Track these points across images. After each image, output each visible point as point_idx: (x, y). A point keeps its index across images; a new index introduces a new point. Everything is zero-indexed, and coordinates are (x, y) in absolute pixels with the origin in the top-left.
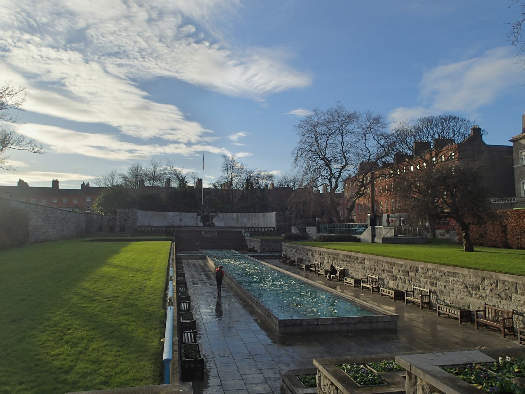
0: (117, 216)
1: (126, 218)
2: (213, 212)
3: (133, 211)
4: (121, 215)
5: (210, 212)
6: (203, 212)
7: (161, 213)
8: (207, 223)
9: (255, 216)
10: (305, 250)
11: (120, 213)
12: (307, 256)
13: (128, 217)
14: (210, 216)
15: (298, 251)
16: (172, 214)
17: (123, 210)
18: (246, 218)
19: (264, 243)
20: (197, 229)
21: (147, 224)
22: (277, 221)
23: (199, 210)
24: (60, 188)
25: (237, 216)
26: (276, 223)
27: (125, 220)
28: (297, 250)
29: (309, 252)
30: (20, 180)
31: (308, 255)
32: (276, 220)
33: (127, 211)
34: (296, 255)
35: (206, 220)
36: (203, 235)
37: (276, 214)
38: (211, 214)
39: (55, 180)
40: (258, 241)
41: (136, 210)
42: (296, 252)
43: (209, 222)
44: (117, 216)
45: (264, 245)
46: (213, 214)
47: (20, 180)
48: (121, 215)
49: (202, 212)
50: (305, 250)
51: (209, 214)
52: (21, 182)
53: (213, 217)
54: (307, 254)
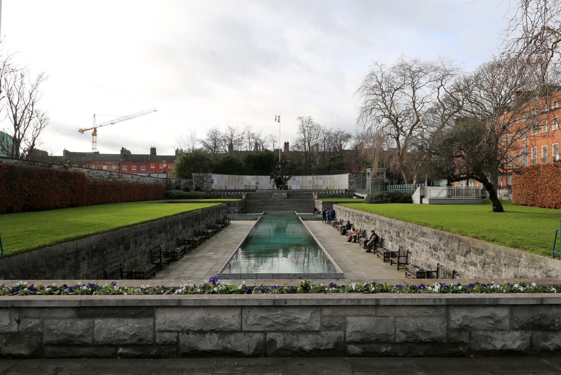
1: (201, 182)
2: (287, 175)
3: (207, 175)
4: (197, 179)
5: (284, 175)
6: (277, 175)
8: (280, 186)
11: (197, 177)
13: (203, 181)
14: (284, 179)
16: (249, 178)
17: (199, 174)
18: (322, 181)
19: (326, 205)
20: (270, 191)
21: (223, 188)
22: (350, 183)
24: (157, 154)
25: (313, 179)
26: (349, 184)
30: (123, 148)
32: (349, 182)
33: (201, 175)
35: (280, 183)
36: (273, 197)
37: (349, 176)
38: (284, 177)
40: (321, 203)
41: (211, 174)
43: (282, 185)
46: (287, 177)
47: (123, 148)
48: (197, 179)
49: (275, 175)
51: (283, 178)
52: (123, 150)
53: (287, 180)
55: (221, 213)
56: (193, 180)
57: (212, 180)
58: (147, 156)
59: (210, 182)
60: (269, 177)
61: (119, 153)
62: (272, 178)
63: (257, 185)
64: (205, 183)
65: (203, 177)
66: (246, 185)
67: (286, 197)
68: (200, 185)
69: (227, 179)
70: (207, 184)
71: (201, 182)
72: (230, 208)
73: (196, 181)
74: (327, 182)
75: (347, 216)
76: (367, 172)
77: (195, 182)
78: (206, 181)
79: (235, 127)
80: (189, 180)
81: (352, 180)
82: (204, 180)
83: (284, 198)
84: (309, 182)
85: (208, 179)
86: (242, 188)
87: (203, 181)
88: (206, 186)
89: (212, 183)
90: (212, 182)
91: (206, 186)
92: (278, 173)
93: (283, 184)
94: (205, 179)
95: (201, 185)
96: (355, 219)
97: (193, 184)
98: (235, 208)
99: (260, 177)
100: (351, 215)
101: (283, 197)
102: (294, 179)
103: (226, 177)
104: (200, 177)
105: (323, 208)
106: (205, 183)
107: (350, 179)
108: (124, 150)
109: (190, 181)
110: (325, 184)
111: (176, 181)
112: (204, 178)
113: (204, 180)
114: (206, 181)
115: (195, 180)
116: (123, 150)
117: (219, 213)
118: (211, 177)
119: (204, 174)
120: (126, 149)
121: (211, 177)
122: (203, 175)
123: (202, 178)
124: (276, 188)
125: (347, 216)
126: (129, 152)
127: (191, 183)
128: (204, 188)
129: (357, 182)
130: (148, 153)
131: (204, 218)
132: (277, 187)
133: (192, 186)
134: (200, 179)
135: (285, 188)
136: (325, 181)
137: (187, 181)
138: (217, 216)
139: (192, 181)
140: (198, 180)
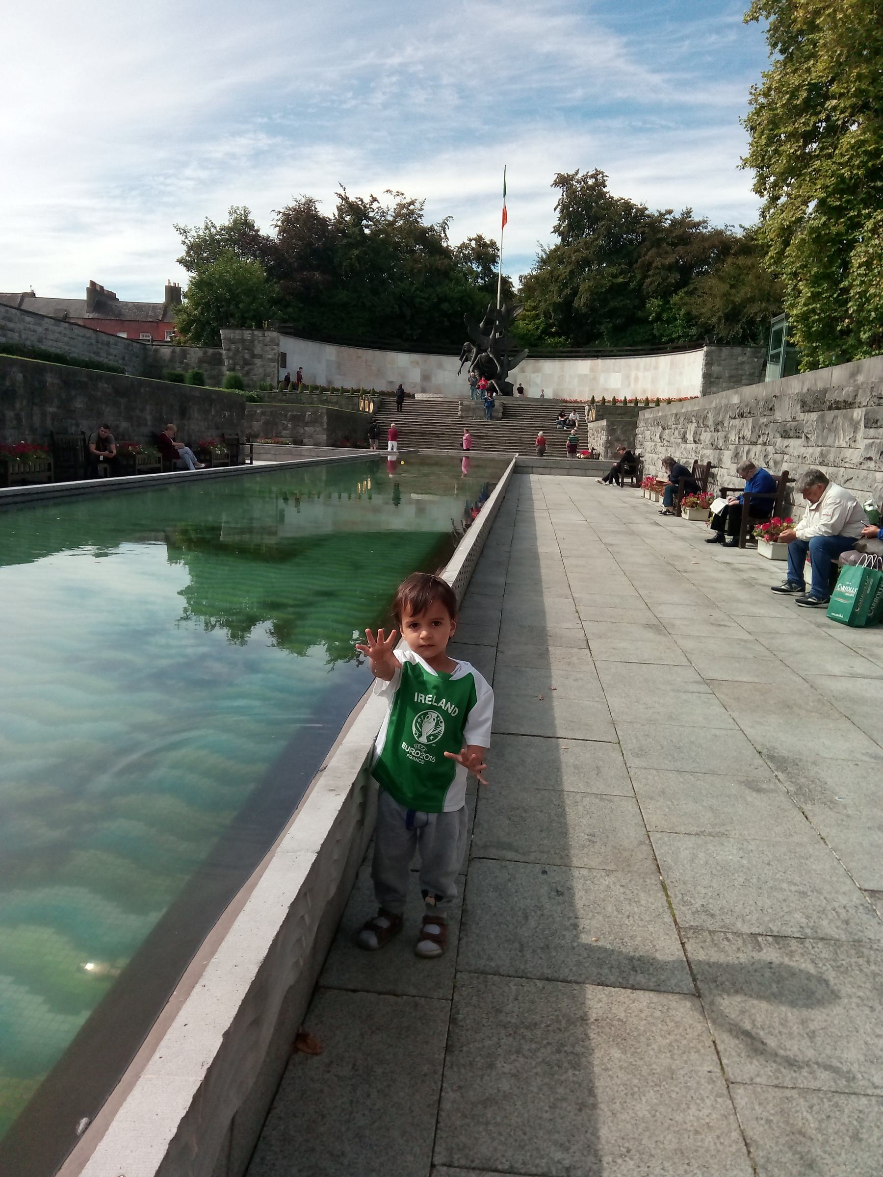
0: (221, 351)
1: (247, 356)
3: (264, 336)
9: (646, 369)
11: (232, 341)
12: (683, 445)
13: (254, 356)
17: (238, 332)
25: (592, 370)
27: (246, 363)
30: (93, 284)
33: (247, 334)
36: (459, 413)
37: (707, 355)
39: (172, 285)
44: (221, 351)
45: (618, 440)
47: (93, 284)
48: (233, 347)
52: (95, 291)
54: (684, 439)
57: (283, 356)
58: (154, 306)
59: (272, 360)
61: (83, 296)
62: (466, 360)
64: (258, 362)
65: (252, 341)
66: (391, 383)
68: (242, 367)
70: (263, 366)
72: (302, 431)
73: (231, 354)
74: (637, 379)
75: (690, 437)
76: (773, 329)
78: (260, 357)
79: (367, 200)
80: (210, 351)
81: (715, 368)
84: (582, 378)
85: (268, 348)
91: (261, 370)
94: (258, 350)
95: (246, 369)
97: (220, 362)
99: (433, 359)
100: (710, 422)
102: (537, 371)
103: (330, 352)
104: (243, 341)
105: (607, 441)
106: (258, 362)
107: (708, 364)
108: (98, 289)
109: (214, 354)
110: (629, 385)
111: (173, 352)
114: (260, 357)
115: (229, 350)
116: (95, 291)
119: (256, 333)
120: (102, 287)
122: (253, 334)
123: (249, 346)
125: (690, 437)
126: (112, 296)
127: (217, 360)
128: (255, 378)
129: (731, 377)
130: (160, 298)
133: (220, 370)
136: (628, 377)
137: (205, 353)
139: (221, 354)
140: (237, 350)
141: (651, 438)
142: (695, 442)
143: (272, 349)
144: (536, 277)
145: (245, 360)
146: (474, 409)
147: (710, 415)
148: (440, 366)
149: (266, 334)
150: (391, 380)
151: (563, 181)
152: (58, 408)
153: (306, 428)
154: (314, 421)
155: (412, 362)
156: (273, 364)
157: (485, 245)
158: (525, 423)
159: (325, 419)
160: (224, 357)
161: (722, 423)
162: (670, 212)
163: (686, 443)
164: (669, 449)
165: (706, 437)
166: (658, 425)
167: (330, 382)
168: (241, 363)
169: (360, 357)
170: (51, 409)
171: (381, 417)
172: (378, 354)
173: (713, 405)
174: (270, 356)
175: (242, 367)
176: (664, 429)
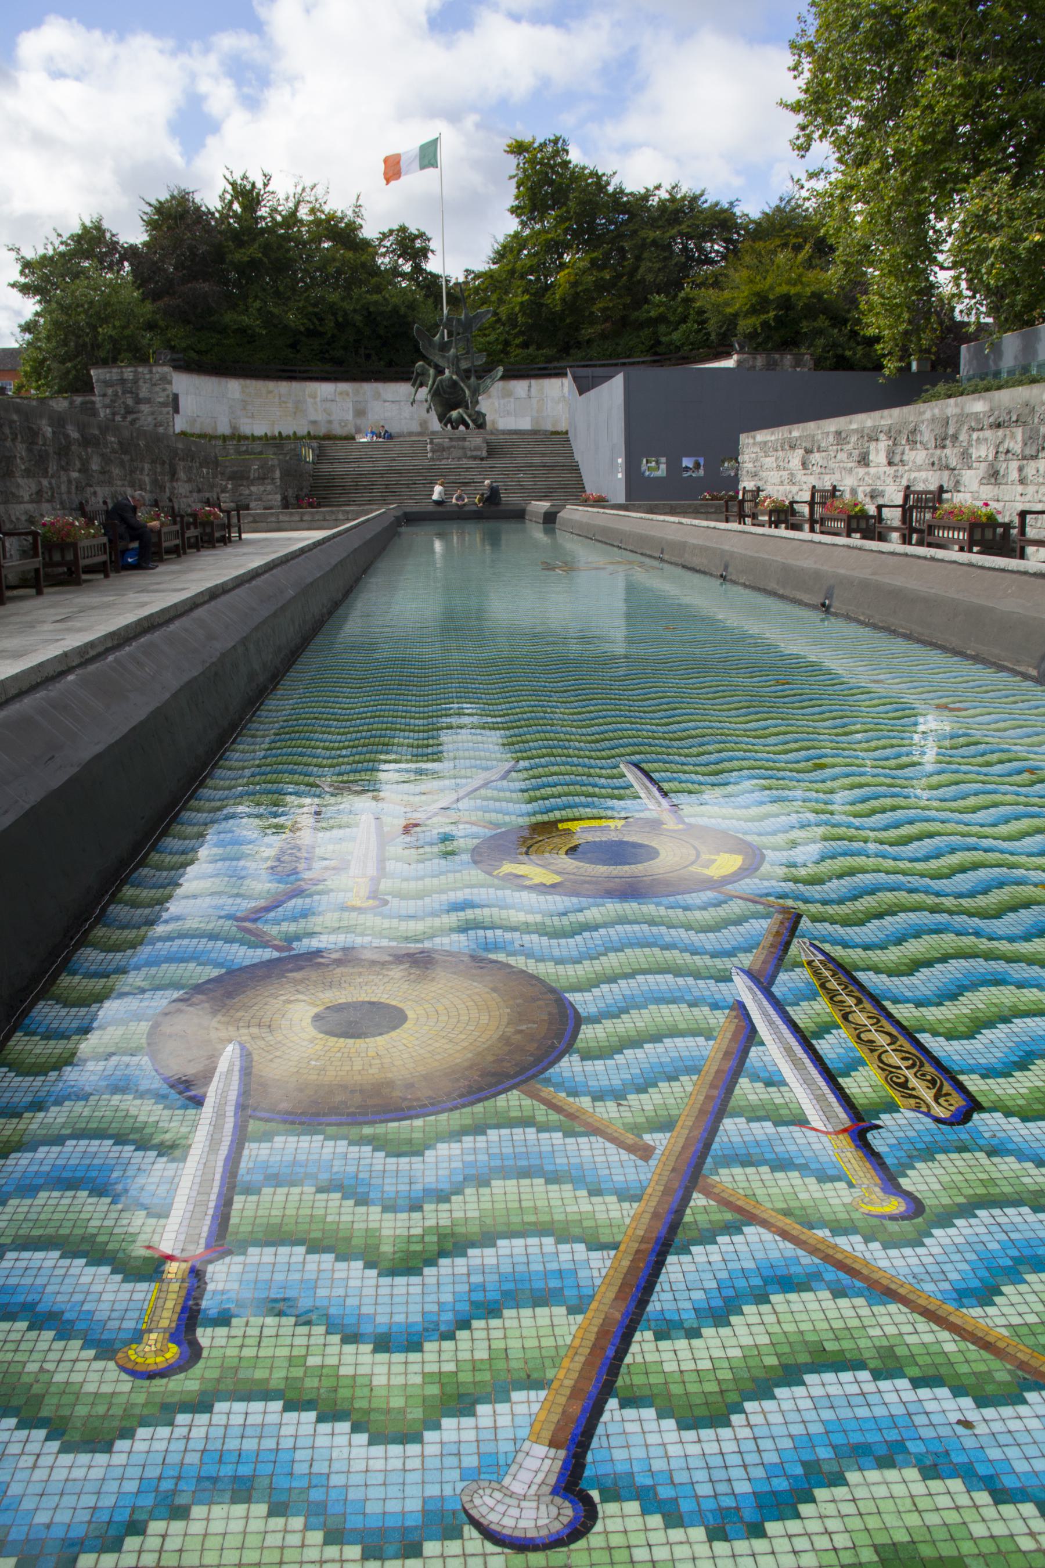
1: (130, 402)
3: (151, 372)
4: (110, 391)
7: (283, 387)
8: (454, 414)
10: (853, 439)
11: (107, 384)
12: (861, 471)
13: (138, 401)
15: (816, 457)
16: (325, 389)
17: (115, 370)
21: (224, 429)
23: (420, 363)
27: (129, 411)
28: (808, 451)
29: (873, 445)
31: (867, 465)
33: (128, 373)
34: (804, 479)
36: (429, 455)
42: (804, 465)
43: (460, 410)
48: (110, 391)
49: (432, 371)
50: (853, 439)
53: (476, 392)
54: (864, 460)
55: (182, 475)
56: (97, 399)
57: (176, 397)
59: (164, 405)
60: (403, 389)
62: (421, 385)
63: (359, 422)
64: (145, 408)
65: (136, 381)
66: (314, 423)
67: (484, 454)
68: (124, 418)
69: (237, 395)
70: (153, 414)
71: (130, 402)
73: (107, 401)
77: (105, 407)
78: (148, 401)
80: (79, 400)
82: (141, 395)
83: (475, 458)
85: (157, 389)
86: (302, 431)
87: (138, 401)
88: (150, 419)
89: (177, 410)
90: (174, 403)
91: (150, 419)
92: (442, 363)
93: (467, 408)
94: (143, 393)
96: (965, 455)
98: (269, 488)
99: (368, 388)
101: (469, 453)
102: (508, 394)
103: (234, 387)
104: (123, 381)
106: (145, 408)
109: (83, 403)
112: (138, 388)
113: (141, 395)
114: (148, 401)
115: (105, 395)
117: (173, 475)
118: (166, 380)
119: (140, 369)
121: (170, 383)
122: (136, 372)
123: (130, 388)
124: (435, 425)
131: (52, 467)
132: (443, 418)
134: (124, 393)
135: (473, 421)
137: (72, 403)
138: (156, 484)
139: (93, 403)
140: (116, 394)
141: (778, 467)
142: (890, 464)
143: (164, 390)
144: (488, 275)
145: (127, 407)
146: (449, 448)
147: (923, 428)
148: (377, 396)
149: (154, 369)
150: (312, 418)
151: (519, 148)
152: (80, 471)
153: (252, 488)
154: (262, 479)
155: (341, 394)
156: (165, 410)
157: (413, 238)
158: (520, 461)
159: (277, 474)
160: (98, 405)
161: (955, 437)
162: (658, 187)
163: (867, 465)
164: (827, 478)
165: (918, 456)
166: (792, 447)
167: (234, 428)
168: (123, 411)
169: (270, 392)
170: (75, 475)
171: (325, 468)
172: (296, 386)
173: (928, 415)
174: (161, 400)
175: (124, 418)
176: (808, 451)
